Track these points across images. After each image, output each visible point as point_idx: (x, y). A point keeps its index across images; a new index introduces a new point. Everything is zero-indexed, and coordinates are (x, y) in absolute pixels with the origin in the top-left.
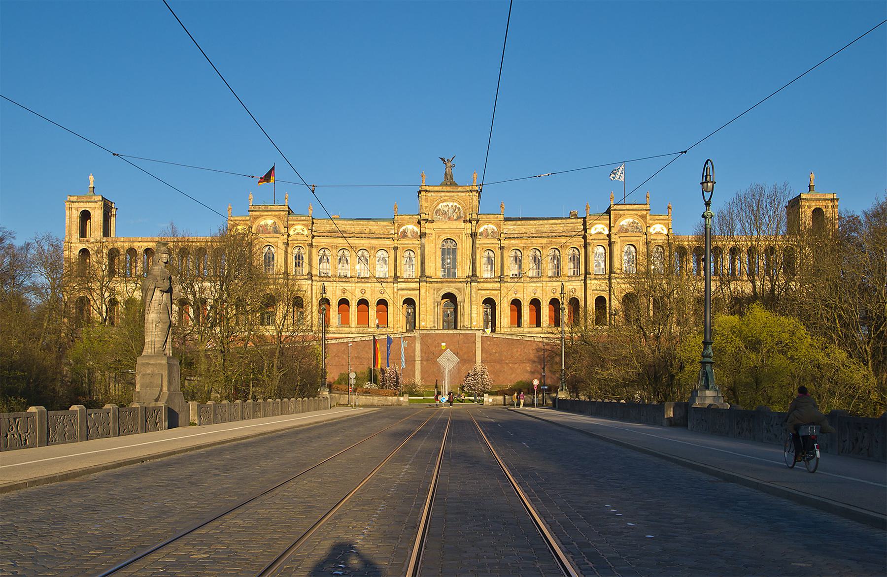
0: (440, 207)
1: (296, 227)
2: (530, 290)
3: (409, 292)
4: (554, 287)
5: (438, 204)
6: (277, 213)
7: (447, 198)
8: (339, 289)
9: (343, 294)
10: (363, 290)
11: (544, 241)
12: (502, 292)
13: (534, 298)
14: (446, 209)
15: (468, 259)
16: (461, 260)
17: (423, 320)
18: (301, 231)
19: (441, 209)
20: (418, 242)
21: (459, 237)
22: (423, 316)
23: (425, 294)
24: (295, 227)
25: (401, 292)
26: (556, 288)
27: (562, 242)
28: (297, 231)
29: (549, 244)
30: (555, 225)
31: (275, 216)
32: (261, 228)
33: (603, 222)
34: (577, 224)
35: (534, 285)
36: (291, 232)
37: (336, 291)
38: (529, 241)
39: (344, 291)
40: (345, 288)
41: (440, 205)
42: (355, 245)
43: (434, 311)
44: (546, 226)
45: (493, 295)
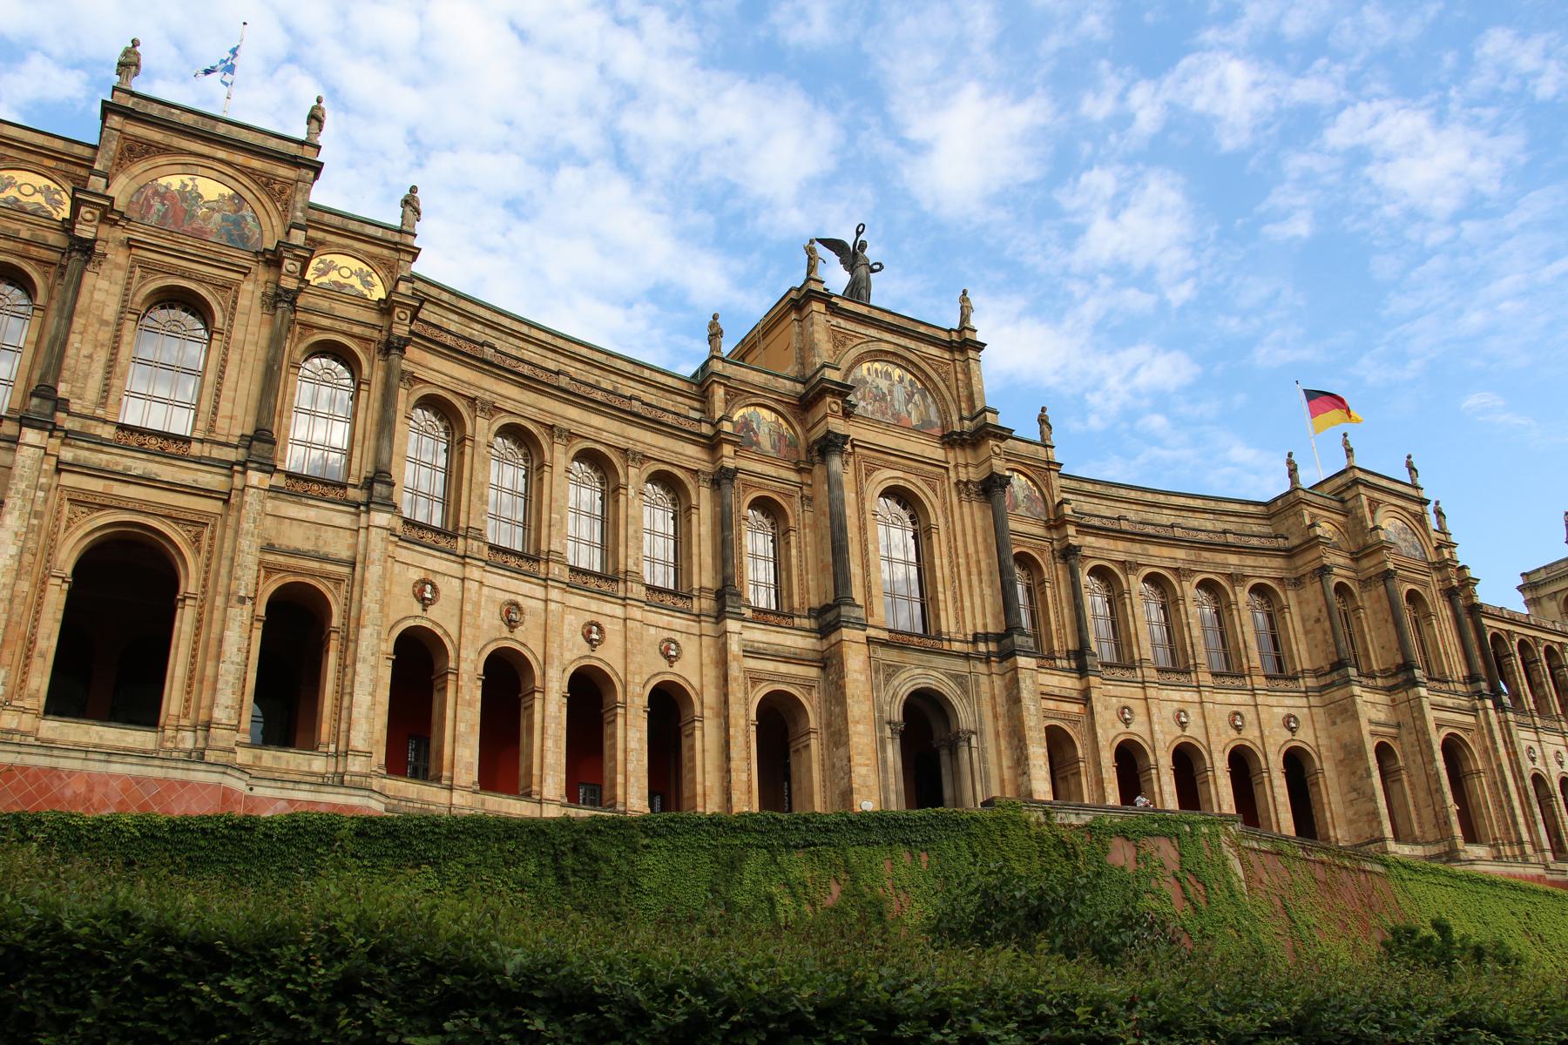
0: (865, 372)
1: (339, 260)
2: (1169, 710)
3: (783, 668)
4: (1235, 709)
5: (859, 360)
6: (256, 163)
7: (885, 347)
8: (491, 599)
9: (505, 629)
10: (595, 629)
11: (1180, 554)
12: (1098, 707)
13: (1183, 740)
14: (884, 384)
15: (974, 570)
16: (947, 571)
17: (864, 790)
18: (356, 282)
19: (869, 379)
20: (793, 476)
21: (934, 490)
22: (863, 770)
23: (863, 678)
24: (328, 258)
25: (752, 663)
26: (1241, 709)
27: (1230, 562)
28: (333, 276)
29: (1194, 562)
30: (1190, 514)
31: (243, 170)
32: (156, 204)
33: (1334, 516)
34: (1249, 520)
35: (1176, 695)
36: (308, 276)
37: (477, 605)
38: (1137, 548)
39: (512, 614)
40: (520, 599)
41: (865, 366)
42: (564, 425)
43: (885, 761)
44: (1165, 511)
45: (1066, 717)
